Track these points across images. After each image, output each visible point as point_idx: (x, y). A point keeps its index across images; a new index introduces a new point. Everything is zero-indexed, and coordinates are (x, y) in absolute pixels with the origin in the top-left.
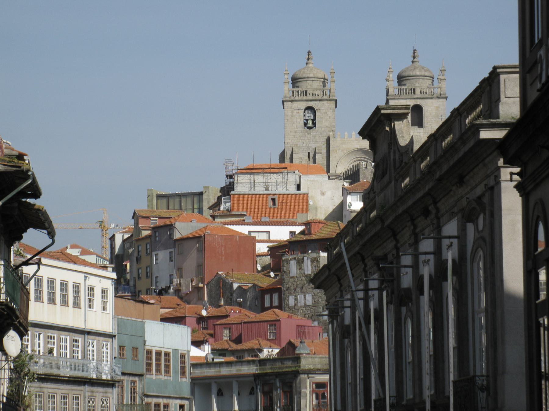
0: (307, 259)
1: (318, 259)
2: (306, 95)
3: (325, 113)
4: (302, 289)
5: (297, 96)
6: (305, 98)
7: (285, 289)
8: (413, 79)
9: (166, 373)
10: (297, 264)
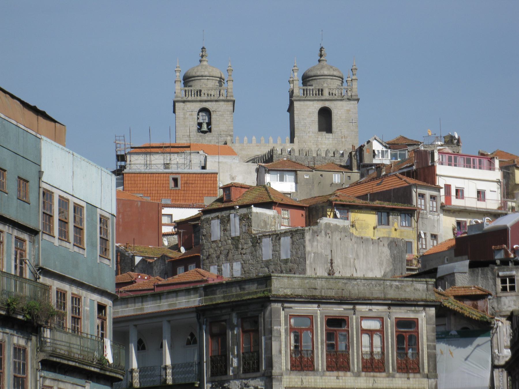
0: (235, 217)
1: (248, 216)
2: (200, 95)
4: (228, 256)
5: (190, 96)
6: (199, 98)
7: (205, 258)
8: (320, 79)
9: (77, 243)
10: (220, 223)
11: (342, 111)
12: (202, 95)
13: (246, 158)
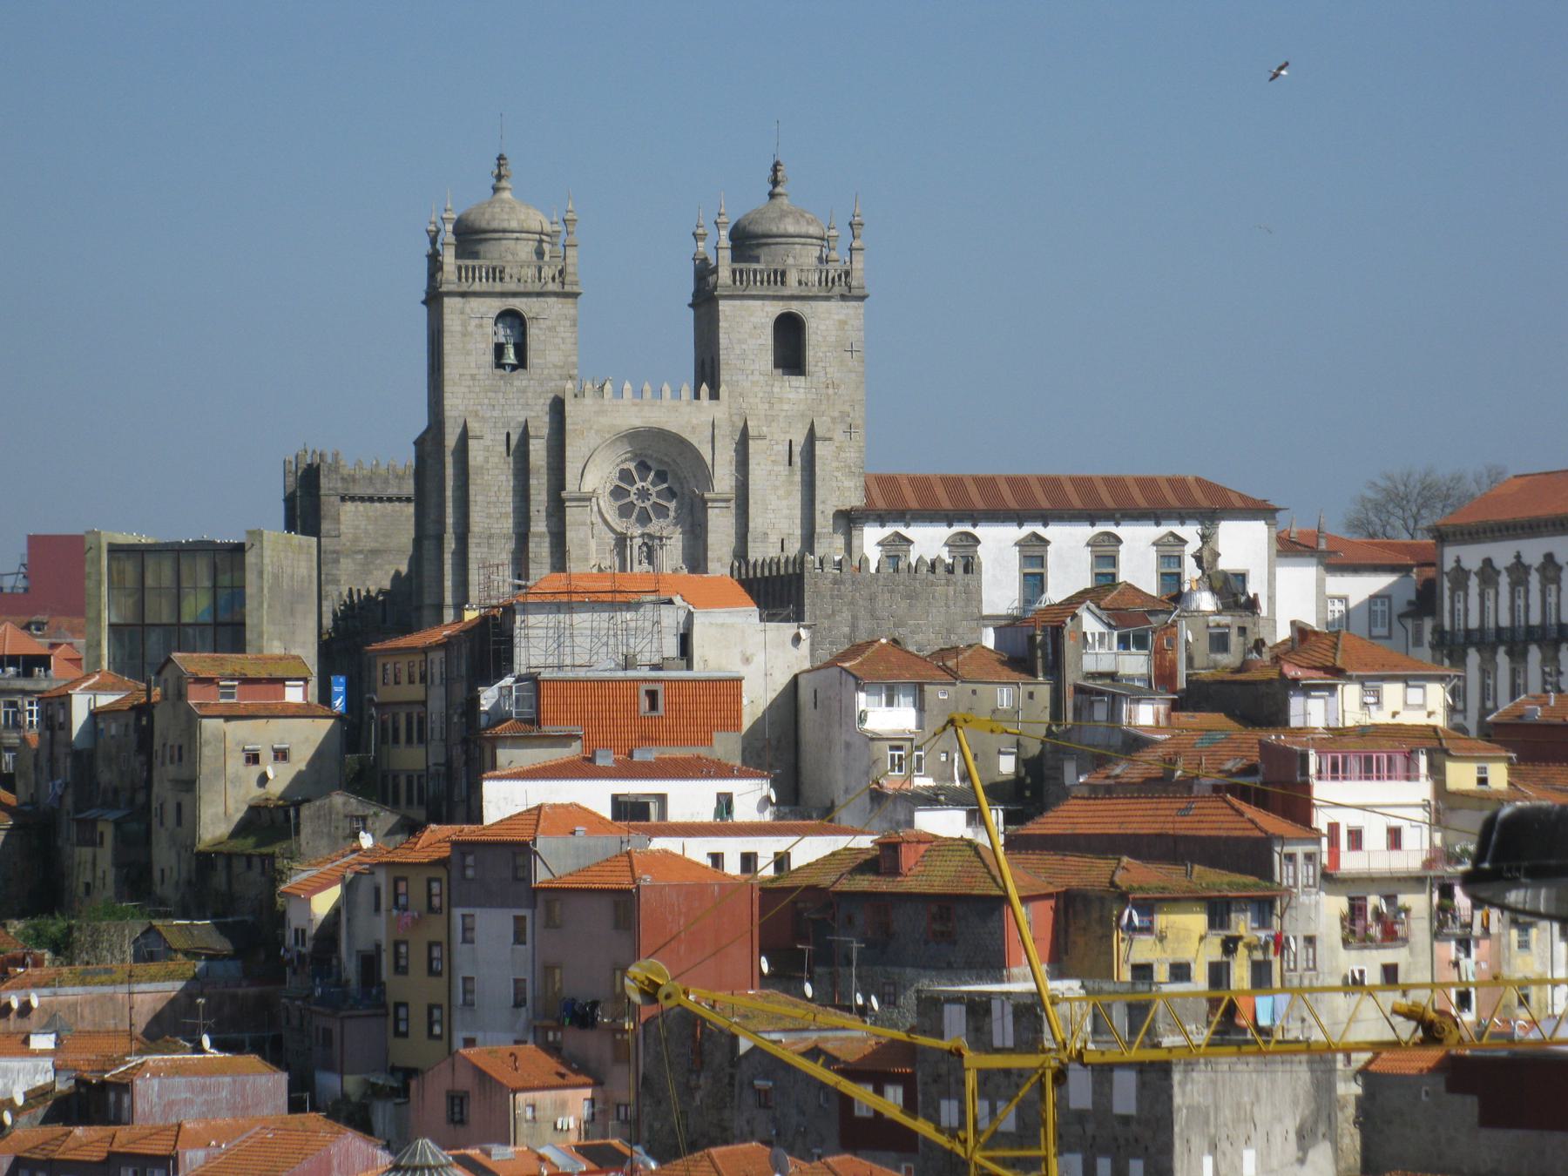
2: (501, 279)
3: (551, 329)
5: (477, 280)
6: (498, 287)
8: (777, 244)
11: (827, 322)
12: (507, 278)
13: (609, 432)
